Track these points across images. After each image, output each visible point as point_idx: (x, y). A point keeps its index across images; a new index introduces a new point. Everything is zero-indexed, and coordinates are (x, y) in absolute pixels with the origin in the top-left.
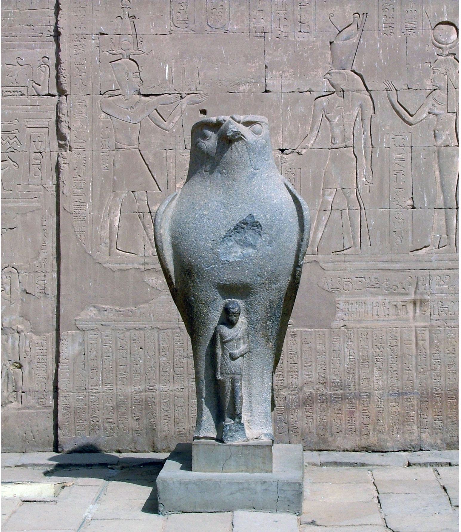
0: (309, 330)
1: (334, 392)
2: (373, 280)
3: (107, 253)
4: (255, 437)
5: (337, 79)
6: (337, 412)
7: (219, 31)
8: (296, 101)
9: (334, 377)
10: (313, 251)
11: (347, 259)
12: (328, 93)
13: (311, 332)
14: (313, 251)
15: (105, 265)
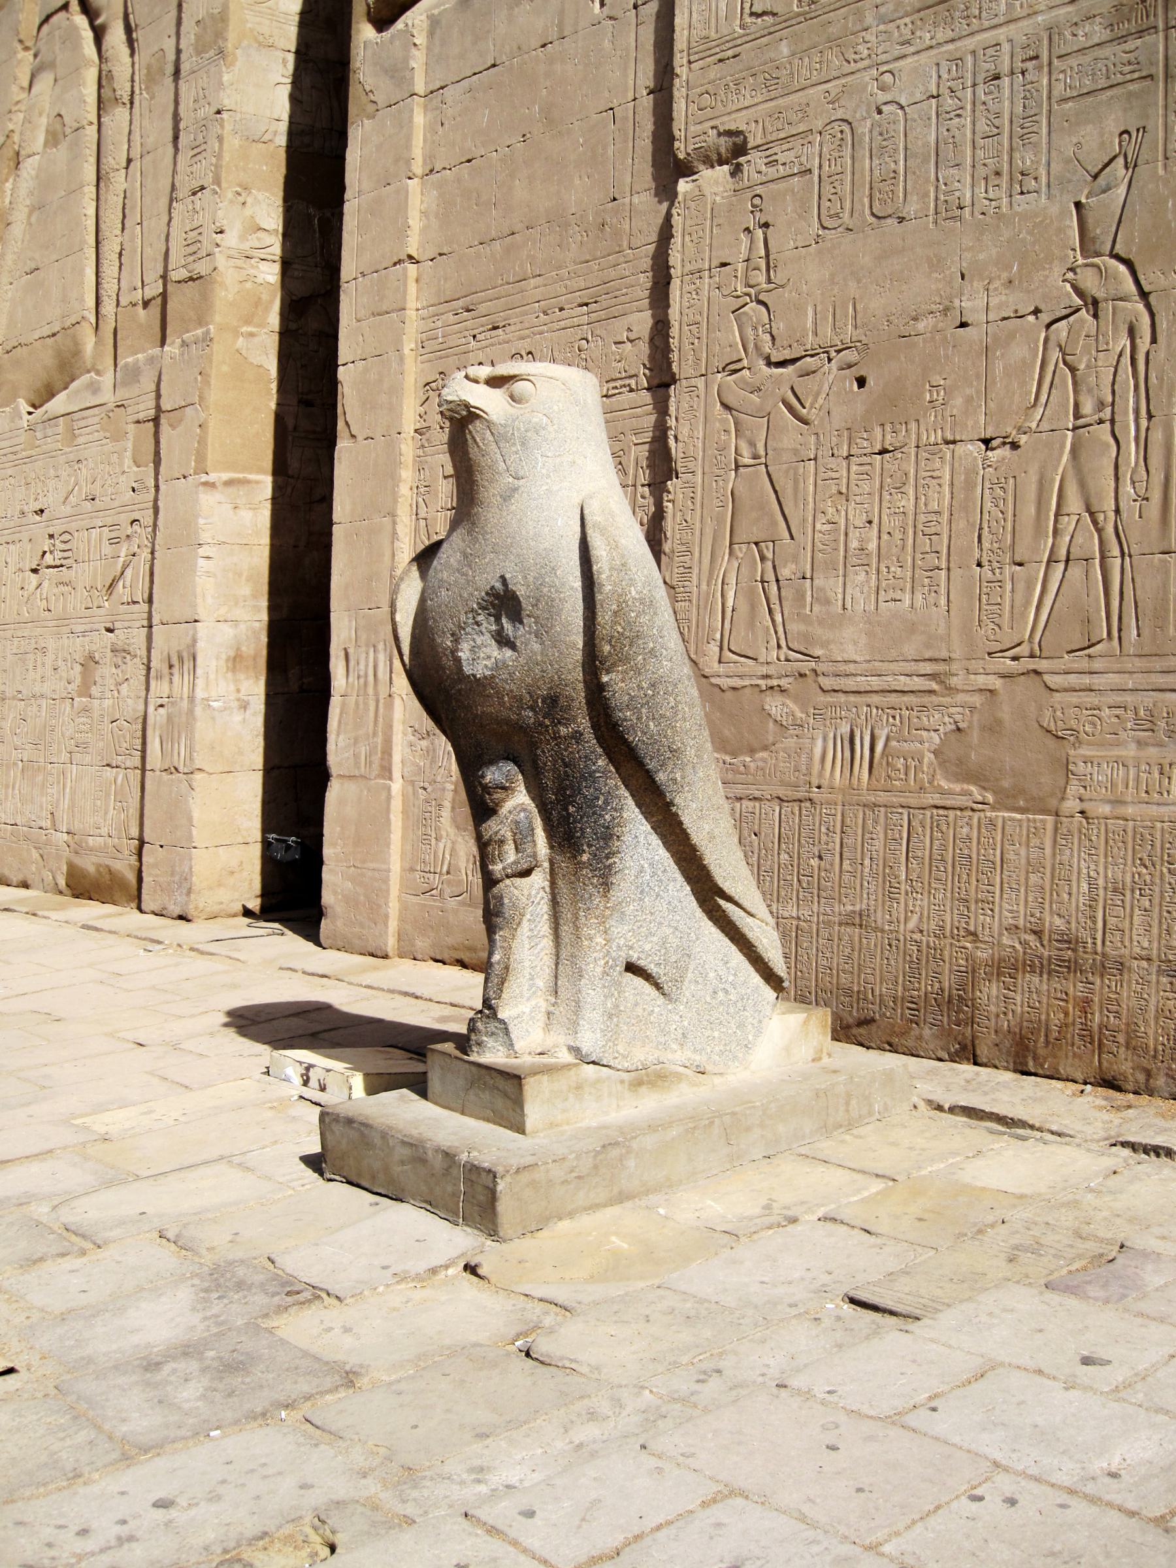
0: (1018, 816)
1: (1057, 952)
2: (1142, 713)
3: (716, 658)
4: (539, 1050)
5: (1090, 282)
6: (1059, 995)
7: (889, 221)
8: (1012, 336)
9: (1058, 921)
10: (1032, 649)
11: (1097, 665)
12: (1068, 311)
13: (1020, 820)
14: (1032, 649)
15: (713, 680)
